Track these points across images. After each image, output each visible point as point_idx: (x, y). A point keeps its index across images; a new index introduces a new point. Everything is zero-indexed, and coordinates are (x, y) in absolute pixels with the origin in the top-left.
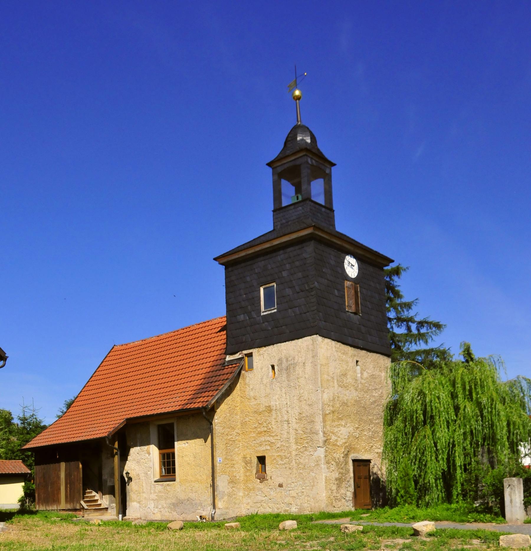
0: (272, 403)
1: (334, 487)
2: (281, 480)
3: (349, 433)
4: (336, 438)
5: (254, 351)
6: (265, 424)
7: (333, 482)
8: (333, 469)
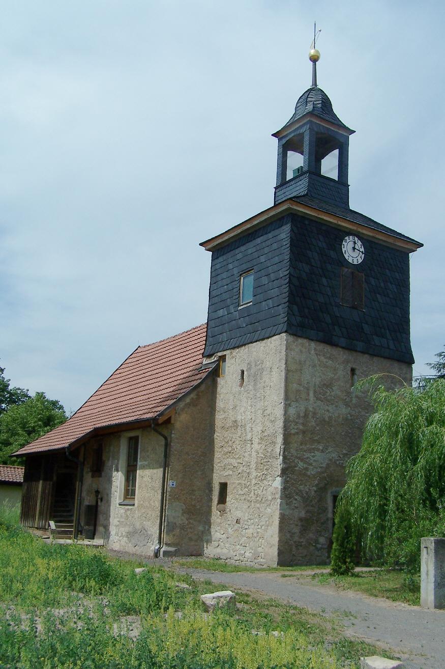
0: (238, 417)
1: (296, 530)
2: (239, 514)
3: (331, 460)
4: (305, 466)
5: (227, 353)
6: (230, 443)
7: (296, 523)
8: (296, 505)
